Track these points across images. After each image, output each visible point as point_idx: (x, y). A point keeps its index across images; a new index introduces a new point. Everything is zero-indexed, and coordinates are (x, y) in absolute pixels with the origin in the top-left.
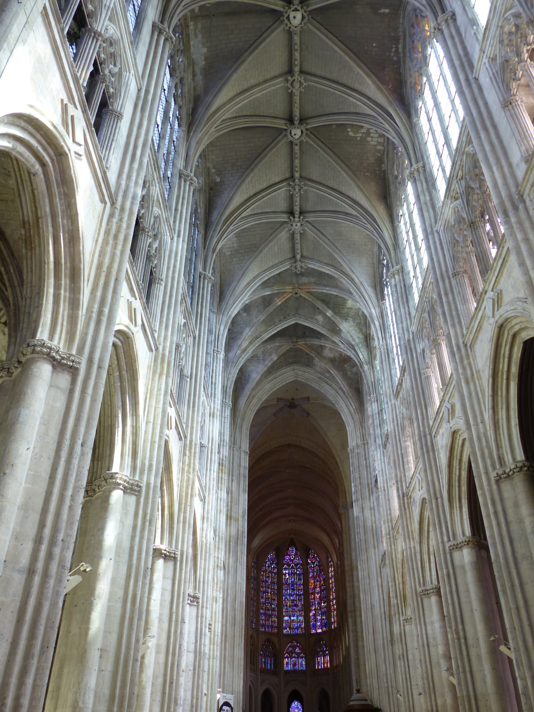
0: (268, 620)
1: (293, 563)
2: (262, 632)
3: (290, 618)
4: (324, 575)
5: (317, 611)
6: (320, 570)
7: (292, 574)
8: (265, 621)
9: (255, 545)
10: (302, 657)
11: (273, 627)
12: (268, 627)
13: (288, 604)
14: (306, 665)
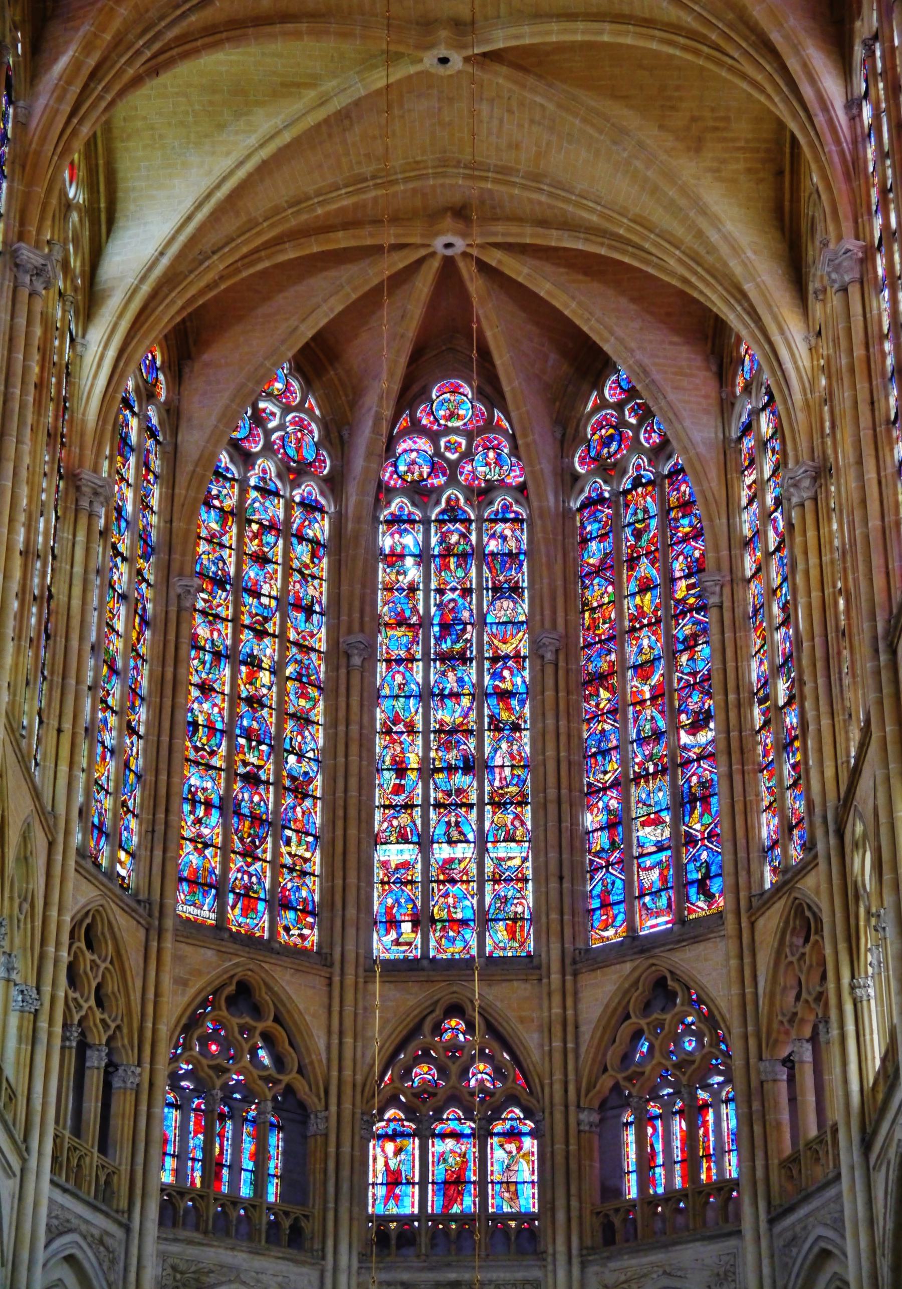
0: (249, 854)
1: (452, 480)
2: (192, 927)
3: (425, 843)
4: (697, 534)
5: (637, 792)
6: (665, 511)
7: (447, 552)
8: (226, 850)
9: (149, 251)
10: (513, 1135)
11: (287, 905)
12: (247, 896)
13: (413, 761)
14: (544, 1184)
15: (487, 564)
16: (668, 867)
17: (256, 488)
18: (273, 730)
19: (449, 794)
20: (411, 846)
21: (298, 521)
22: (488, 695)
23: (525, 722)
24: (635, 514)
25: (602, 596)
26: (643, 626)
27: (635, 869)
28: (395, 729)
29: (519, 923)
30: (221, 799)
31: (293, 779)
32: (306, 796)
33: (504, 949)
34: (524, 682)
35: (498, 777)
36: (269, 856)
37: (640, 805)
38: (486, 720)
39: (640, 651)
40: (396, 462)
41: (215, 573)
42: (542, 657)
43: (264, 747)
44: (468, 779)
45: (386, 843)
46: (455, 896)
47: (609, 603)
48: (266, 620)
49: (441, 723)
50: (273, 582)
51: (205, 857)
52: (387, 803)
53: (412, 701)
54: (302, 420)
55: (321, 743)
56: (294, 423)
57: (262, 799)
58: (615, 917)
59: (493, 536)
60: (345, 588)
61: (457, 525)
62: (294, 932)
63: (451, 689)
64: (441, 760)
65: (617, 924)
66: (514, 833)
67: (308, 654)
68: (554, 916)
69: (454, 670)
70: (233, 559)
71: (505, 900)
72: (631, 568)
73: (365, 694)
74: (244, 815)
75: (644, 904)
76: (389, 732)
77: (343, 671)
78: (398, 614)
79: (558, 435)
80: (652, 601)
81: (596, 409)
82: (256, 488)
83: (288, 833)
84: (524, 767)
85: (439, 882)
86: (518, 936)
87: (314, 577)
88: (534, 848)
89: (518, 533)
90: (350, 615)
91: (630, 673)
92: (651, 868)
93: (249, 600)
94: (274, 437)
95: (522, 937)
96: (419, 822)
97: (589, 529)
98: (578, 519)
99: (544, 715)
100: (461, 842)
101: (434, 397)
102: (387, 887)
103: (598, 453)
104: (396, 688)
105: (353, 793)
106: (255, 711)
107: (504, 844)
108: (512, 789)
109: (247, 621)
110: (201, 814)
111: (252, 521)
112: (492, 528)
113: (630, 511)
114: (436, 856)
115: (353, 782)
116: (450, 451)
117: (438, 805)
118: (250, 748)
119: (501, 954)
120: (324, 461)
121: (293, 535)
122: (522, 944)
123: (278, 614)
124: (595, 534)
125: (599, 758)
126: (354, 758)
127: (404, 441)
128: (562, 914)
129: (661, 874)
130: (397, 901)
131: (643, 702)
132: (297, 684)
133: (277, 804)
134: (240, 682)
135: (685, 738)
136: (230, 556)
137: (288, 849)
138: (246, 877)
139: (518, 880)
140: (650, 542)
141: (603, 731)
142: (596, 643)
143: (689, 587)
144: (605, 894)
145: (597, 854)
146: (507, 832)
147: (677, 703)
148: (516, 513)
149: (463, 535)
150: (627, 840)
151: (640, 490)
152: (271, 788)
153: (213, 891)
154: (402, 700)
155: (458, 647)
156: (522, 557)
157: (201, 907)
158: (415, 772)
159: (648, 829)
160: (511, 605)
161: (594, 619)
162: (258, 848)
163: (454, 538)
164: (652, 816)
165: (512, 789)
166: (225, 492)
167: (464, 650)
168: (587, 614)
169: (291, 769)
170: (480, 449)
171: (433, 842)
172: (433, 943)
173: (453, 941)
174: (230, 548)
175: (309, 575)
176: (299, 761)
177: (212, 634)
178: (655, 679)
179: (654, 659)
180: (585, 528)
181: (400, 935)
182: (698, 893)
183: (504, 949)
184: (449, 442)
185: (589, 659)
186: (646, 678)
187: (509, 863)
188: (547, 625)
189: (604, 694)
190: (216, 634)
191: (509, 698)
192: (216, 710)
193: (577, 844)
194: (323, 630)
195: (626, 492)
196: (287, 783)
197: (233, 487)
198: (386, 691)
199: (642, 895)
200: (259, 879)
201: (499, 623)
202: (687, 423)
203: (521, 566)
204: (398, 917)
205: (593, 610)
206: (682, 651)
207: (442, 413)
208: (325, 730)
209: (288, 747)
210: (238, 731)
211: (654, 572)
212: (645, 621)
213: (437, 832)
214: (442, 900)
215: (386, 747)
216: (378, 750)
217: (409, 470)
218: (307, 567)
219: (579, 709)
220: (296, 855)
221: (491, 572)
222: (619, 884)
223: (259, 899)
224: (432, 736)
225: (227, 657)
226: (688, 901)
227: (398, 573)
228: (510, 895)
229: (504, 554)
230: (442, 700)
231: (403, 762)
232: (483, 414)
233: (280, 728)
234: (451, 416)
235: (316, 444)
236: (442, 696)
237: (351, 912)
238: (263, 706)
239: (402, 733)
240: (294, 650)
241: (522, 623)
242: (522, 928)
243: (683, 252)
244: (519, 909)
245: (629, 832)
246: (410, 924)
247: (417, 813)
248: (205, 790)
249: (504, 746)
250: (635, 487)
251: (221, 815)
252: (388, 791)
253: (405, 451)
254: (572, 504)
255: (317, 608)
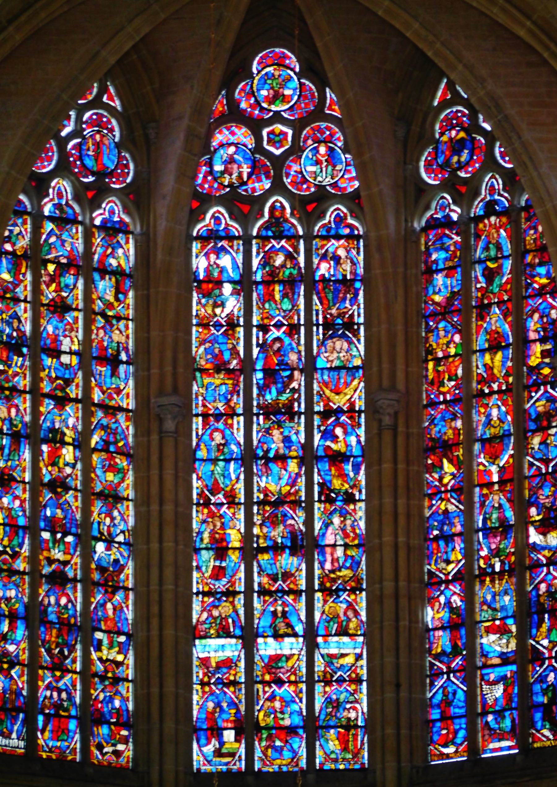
11: (100, 720)
15: (318, 294)
16: (513, 684)
17: (51, 219)
18: (78, 516)
19: (274, 578)
20: (234, 641)
21: (100, 250)
22: (319, 459)
23: (360, 492)
24: (486, 248)
25: (449, 343)
26: (492, 393)
27: (478, 681)
28: (213, 500)
29: (353, 731)
30: (26, 607)
31: (102, 569)
32: (116, 589)
33: (335, 761)
34: (359, 442)
35: (329, 558)
36: (78, 666)
37: (485, 607)
38: (316, 488)
39: (489, 423)
40: (211, 159)
41: (10, 336)
42: (380, 421)
43: (69, 539)
44: (295, 561)
45: (205, 637)
46: (282, 699)
47: (456, 355)
48: (68, 382)
49: (265, 491)
50: (73, 334)
51: (12, 678)
52: (206, 589)
53: (232, 465)
54: (100, 116)
55: (131, 522)
56: (91, 123)
57: (69, 601)
58: (456, 732)
59: (324, 257)
60: (154, 334)
61: (283, 242)
62: (108, 749)
63: (277, 451)
64: (266, 537)
65: (459, 741)
66: (347, 625)
67: (114, 415)
68: (390, 731)
69: (280, 427)
70: (28, 315)
71: (336, 705)
72: (481, 317)
73: (180, 464)
74: (52, 623)
75: (487, 723)
76: (207, 503)
77: (155, 437)
78: (215, 357)
79: (401, 133)
80: (503, 363)
81: (444, 104)
82: (51, 219)
83: (99, 635)
84: (358, 546)
85: (264, 683)
86: (351, 747)
87: (119, 318)
88: (369, 643)
89: (354, 252)
90: (161, 366)
91: (477, 447)
92: (495, 683)
93: (48, 361)
94: (69, 146)
95: (355, 746)
96: (241, 612)
97: (434, 257)
98: (423, 241)
99: (380, 488)
100: (288, 635)
101: (255, 71)
102: (207, 689)
103: (447, 162)
104: (215, 449)
105: (169, 586)
106: (59, 496)
107: (336, 639)
108: (344, 572)
109: (46, 387)
110: (6, 629)
111: (49, 261)
112: (323, 246)
113: (481, 244)
114: (261, 652)
115: (169, 573)
116: (274, 145)
117: (263, 592)
118: (55, 541)
119: (333, 766)
120: (127, 166)
121: (96, 270)
122: (356, 754)
123: (80, 374)
124: (441, 266)
125: (442, 543)
126: (169, 545)
127: (220, 132)
128: (398, 727)
129: (505, 690)
130: (218, 705)
131: (490, 485)
132: (104, 455)
133: (86, 603)
134: (42, 464)
135: (534, 537)
136: (25, 311)
137: (99, 654)
138: (55, 694)
139: (352, 681)
140: (501, 286)
141: (446, 511)
142: (441, 403)
143: (544, 354)
144: (447, 703)
145: (437, 657)
146: (340, 624)
147: (527, 492)
148: (351, 227)
149: (290, 257)
150: (471, 645)
151: (493, 219)
152: (79, 586)
153: (21, 716)
154: (221, 464)
155: (284, 398)
156: (358, 285)
157: (8, 737)
158: (237, 552)
159: (493, 637)
160: (345, 345)
161: (438, 372)
162: (66, 658)
163: (279, 260)
164: (498, 623)
165: (344, 572)
166: (17, 230)
167: (291, 401)
168: (431, 365)
169: (99, 559)
170: (310, 142)
171: (258, 635)
172: (258, 753)
173: (280, 750)
174: (25, 301)
175: (113, 317)
176: (108, 549)
177: (9, 412)
178: (504, 460)
179: (504, 435)
180: (430, 255)
181: (222, 744)
182: (543, 719)
183: (335, 761)
184: (272, 132)
185: (432, 422)
186: (494, 457)
187: (342, 661)
188: (386, 383)
189: (448, 467)
190: (13, 411)
191: (342, 461)
192: (17, 503)
193: (416, 644)
194: (131, 383)
195: (478, 219)
196: (96, 576)
197: (25, 222)
198: (202, 454)
199: (485, 713)
200: (69, 694)
201: (330, 369)
202: (544, 169)
203: (356, 295)
204: (220, 723)
205: (438, 361)
206: (534, 432)
207: (264, 93)
208: (136, 507)
209: (95, 533)
210: (42, 524)
211: (507, 326)
212: (495, 387)
213: (262, 624)
214: (268, 704)
215: (204, 522)
216: (195, 525)
217: (227, 171)
218: (110, 306)
219: (420, 481)
220: (108, 660)
221: (321, 303)
222: (460, 695)
223: (70, 717)
224: (255, 508)
225: (27, 437)
226: (533, 726)
227: (215, 305)
228: (342, 697)
229: (337, 281)
230: (266, 465)
231: (223, 538)
232: (313, 95)
233: (87, 512)
234: (276, 97)
235: (117, 145)
236: (268, 460)
237: (169, 725)
238: (67, 489)
239: (222, 504)
240: (100, 414)
241: (357, 368)
242: (355, 736)
243: (534, 23)
244: (353, 715)
245: (472, 636)
246: (233, 732)
247: (240, 601)
248: (8, 599)
249: (336, 520)
250: (487, 215)
251: (27, 627)
252: (206, 575)
253: (221, 145)
254: (416, 225)
255: (123, 357)
